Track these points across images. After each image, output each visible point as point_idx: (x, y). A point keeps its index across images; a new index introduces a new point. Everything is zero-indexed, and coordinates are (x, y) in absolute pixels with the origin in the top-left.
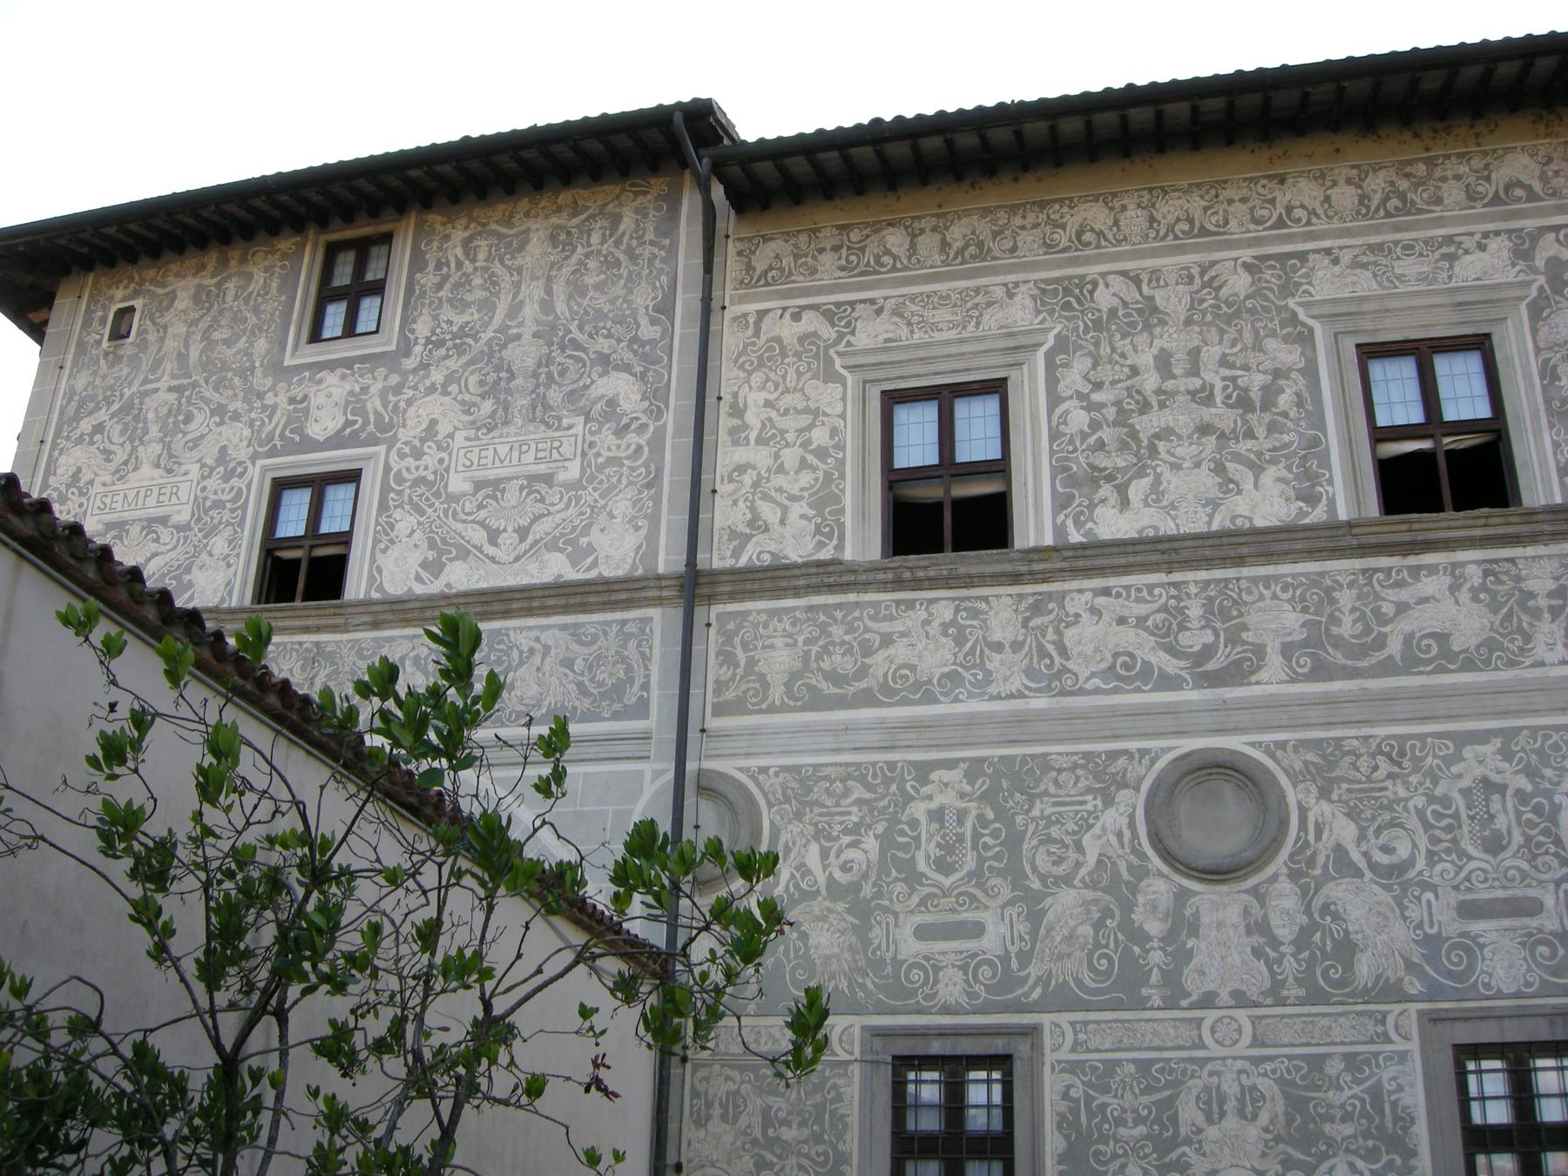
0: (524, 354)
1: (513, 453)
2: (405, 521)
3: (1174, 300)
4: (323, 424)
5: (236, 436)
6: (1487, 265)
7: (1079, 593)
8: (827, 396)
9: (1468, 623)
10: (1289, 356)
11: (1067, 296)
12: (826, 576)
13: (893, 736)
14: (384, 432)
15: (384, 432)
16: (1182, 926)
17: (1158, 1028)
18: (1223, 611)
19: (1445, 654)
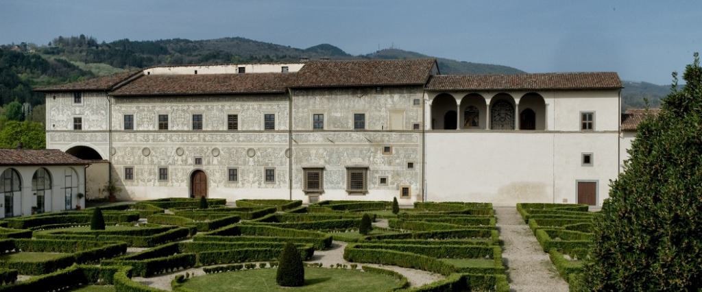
0: (95, 107)
1: (94, 117)
2: (86, 123)
3: (146, 109)
4: (78, 112)
5: (69, 112)
6: (168, 108)
7: (138, 134)
8: (120, 115)
9: (163, 138)
10: (153, 115)
11: (138, 108)
12: (120, 131)
13: (125, 144)
14: (83, 114)
15: (83, 114)
16: (144, 160)
17: (142, 167)
18: (148, 136)
19: (161, 141)
